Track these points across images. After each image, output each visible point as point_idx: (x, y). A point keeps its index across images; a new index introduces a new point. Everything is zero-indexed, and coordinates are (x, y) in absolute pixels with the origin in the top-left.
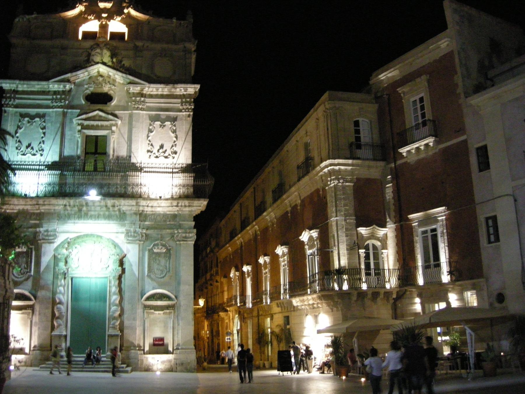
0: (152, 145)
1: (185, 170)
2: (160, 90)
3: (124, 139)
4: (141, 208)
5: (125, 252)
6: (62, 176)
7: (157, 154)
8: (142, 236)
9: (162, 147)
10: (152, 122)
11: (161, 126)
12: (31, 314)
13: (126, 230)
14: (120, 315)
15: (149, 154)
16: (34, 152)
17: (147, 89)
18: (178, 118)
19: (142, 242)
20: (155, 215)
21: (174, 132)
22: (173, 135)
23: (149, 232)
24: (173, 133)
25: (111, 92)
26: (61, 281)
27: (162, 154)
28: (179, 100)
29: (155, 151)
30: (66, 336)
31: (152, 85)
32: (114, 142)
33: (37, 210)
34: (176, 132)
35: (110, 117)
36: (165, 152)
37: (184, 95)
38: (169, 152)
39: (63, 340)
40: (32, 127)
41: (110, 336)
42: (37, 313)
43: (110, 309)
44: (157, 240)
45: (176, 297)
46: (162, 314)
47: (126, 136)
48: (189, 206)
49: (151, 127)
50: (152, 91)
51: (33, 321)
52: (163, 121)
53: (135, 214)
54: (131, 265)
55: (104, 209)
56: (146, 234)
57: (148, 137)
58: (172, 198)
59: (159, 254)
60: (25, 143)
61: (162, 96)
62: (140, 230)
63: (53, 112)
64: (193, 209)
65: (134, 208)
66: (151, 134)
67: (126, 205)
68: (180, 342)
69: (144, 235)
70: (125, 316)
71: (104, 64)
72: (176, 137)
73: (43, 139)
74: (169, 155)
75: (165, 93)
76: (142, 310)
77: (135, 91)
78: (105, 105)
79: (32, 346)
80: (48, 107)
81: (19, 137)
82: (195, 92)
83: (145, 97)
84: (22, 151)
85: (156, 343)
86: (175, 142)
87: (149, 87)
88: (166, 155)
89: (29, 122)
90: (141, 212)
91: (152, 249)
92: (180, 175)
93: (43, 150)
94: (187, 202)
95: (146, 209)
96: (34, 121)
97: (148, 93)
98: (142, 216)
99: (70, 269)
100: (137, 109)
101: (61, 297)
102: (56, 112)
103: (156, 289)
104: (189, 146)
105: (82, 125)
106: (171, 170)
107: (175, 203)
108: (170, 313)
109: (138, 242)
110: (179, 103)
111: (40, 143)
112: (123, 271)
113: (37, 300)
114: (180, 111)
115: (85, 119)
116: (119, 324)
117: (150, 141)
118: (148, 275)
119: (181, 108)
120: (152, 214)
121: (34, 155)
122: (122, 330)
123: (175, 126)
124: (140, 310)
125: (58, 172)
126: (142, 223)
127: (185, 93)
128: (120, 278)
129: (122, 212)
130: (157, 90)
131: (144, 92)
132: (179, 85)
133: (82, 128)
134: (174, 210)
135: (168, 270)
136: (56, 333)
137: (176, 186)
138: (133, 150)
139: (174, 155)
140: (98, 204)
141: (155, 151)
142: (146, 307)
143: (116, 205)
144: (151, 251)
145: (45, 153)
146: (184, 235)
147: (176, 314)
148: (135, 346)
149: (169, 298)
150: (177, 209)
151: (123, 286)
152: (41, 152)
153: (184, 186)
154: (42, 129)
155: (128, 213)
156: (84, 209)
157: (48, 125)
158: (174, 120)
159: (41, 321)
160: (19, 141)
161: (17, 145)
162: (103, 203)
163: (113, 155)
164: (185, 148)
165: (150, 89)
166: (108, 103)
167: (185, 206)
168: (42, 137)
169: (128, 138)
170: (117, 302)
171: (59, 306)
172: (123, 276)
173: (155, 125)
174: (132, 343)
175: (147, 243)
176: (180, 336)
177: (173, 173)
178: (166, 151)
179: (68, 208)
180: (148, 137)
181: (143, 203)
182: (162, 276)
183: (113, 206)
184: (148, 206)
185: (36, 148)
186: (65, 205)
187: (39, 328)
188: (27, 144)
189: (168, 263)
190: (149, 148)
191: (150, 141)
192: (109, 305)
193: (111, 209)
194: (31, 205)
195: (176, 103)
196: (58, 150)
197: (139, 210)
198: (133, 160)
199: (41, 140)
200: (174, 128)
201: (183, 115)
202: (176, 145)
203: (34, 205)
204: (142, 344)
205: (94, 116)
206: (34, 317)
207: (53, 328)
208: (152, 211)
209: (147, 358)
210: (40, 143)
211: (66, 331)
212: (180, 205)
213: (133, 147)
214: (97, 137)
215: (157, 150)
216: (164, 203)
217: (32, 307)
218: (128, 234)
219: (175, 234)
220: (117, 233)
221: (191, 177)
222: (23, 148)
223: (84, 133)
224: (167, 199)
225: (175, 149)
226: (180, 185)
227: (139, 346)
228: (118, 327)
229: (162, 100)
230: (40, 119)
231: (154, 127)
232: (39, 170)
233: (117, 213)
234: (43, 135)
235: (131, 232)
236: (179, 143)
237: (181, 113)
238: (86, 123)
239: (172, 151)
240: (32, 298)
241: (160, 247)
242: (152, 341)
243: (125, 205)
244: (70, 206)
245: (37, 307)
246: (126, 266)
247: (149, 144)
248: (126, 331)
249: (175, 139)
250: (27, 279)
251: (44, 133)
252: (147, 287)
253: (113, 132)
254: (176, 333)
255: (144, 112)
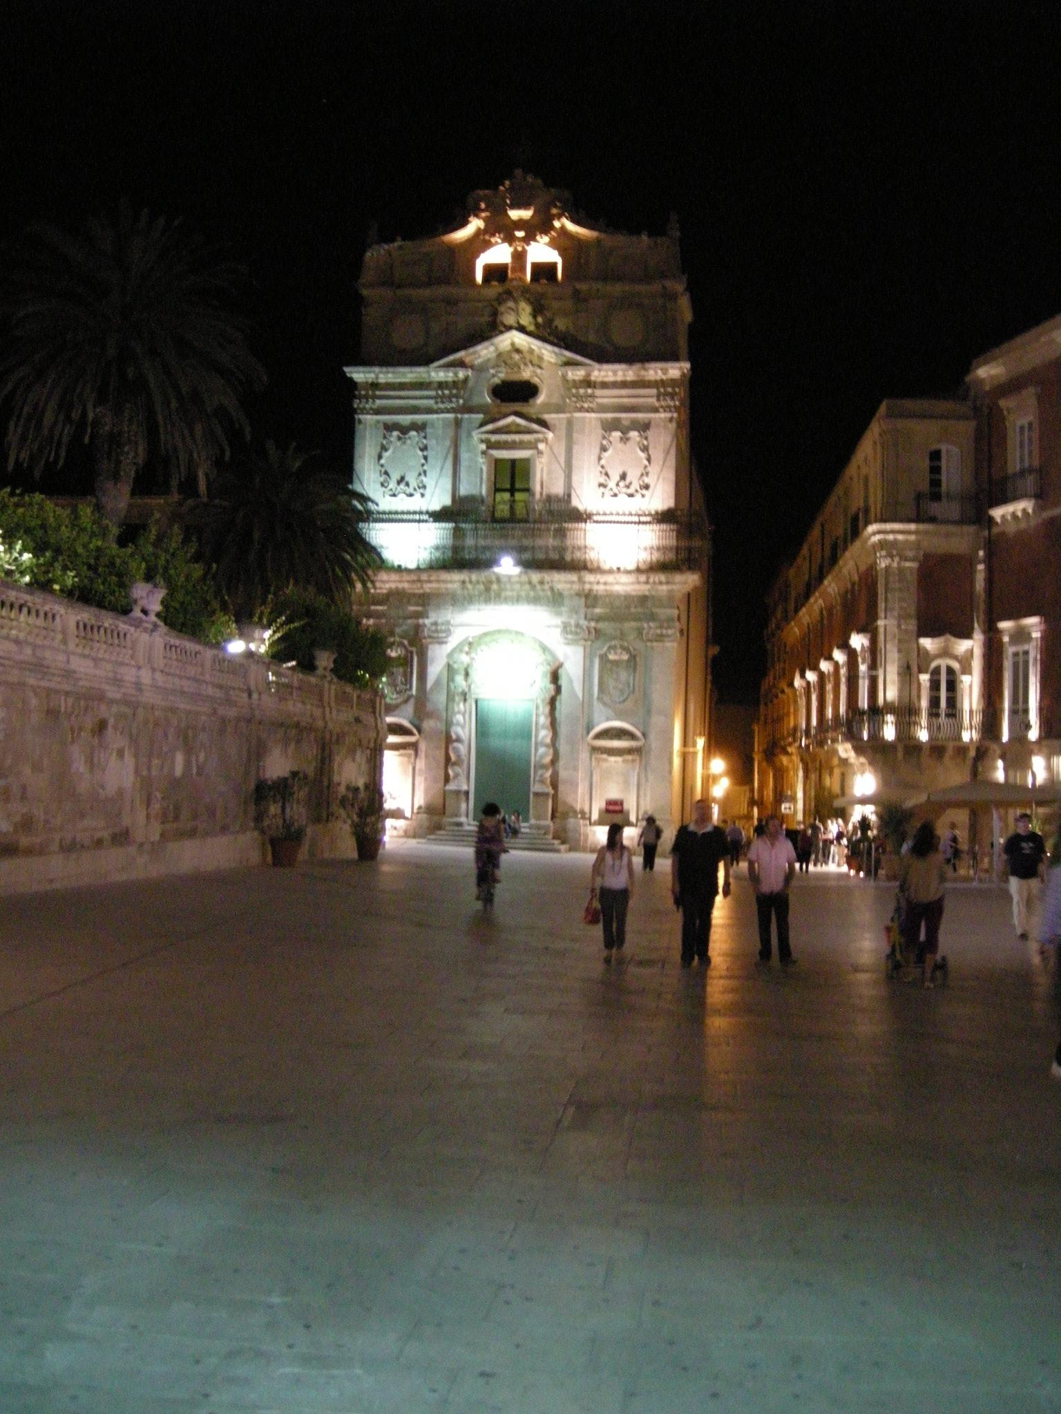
0: (607, 474)
1: (664, 517)
2: (620, 373)
3: (559, 463)
4: (587, 587)
5: (562, 659)
6: (457, 533)
7: (616, 490)
8: (589, 632)
9: (623, 477)
10: (606, 431)
11: (621, 439)
12: (413, 756)
13: (563, 623)
14: (554, 762)
15: (602, 489)
16: (410, 490)
17: (596, 373)
18: (653, 422)
19: (589, 643)
20: (610, 596)
21: (645, 449)
22: (643, 455)
23: (601, 625)
24: (643, 452)
25: (536, 380)
26: (458, 704)
27: (625, 490)
28: (654, 391)
29: (612, 484)
30: (467, 793)
31: (605, 366)
32: (542, 470)
33: (419, 589)
34: (647, 451)
35: (535, 427)
36: (628, 487)
37: (662, 381)
38: (635, 486)
39: (464, 798)
40: (405, 447)
41: (537, 794)
42: (422, 754)
43: (536, 750)
44: (615, 638)
45: (644, 735)
46: (620, 764)
47: (562, 460)
48: (668, 583)
49: (605, 442)
50: (605, 376)
51: (417, 768)
52: (625, 431)
53: (578, 595)
54: (571, 681)
55: (527, 587)
56: (595, 629)
57: (600, 459)
58: (638, 570)
59: (616, 663)
60: (395, 476)
61: (624, 385)
62: (586, 623)
63: (438, 419)
64: (674, 587)
65: (576, 587)
66: (606, 455)
67: (562, 581)
68: (648, 808)
69: (593, 631)
70: (561, 763)
71: (522, 329)
72: (649, 460)
73: (425, 467)
74: (637, 491)
75: (629, 379)
76: (588, 754)
77: (576, 378)
78: (525, 404)
79: (416, 806)
80: (429, 411)
81: (386, 465)
82: (683, 375)
83: (595, 387)
84: (391, 490)
85: (611, 808)
86: (646, 467)
87: (600, 370)
88: (631, 491)
89: (399, 438)
90: (586, 592)
91: (605, 654)
92: (656, 527)
93: (424, 487)
94: (663, 577)
95: (595, 587)
96: (407, 436)
97: (600, 379)
98: (590, 598)
99: (473, 687)
100: (581, 409)
101: (460, 730)
102: (443, 420)
103: (612, 720)
104: (670, 475)
105: (487, 442)
106: (636, 519)
107: (643, 578)
108: (633, 761)
109: (583, 642)
110: (652, 397)
111: (420, 474)
112: (558, 690)
113: (423, 735)
114: (656, 410)
115: (493, 432)
116: (551, 776)
117: (603, 467)
118: (599, 698)
119: (657, 404)
120: (607, 596)
121: (411, 495)
122: (555, 784)
123: (646, 438)
124: (584, 755)
125: (451, 525)
126: (590, 610)
127: (664, 377)
128: (552, 702)
129: (556, 591)
130: (615, 373)
131: (593, 378)
132: (653, 365)
133: (488, 448)
134: (644, 589)
135: (631, 689)
136: (451, 787)
137: (645, 549)
138: (575, 483)
139: (644, 492)
140: (517, 579)
141: (612, 484)
142: (595, 749)
143: (546, 580)
144: (603, 658)
145: (428, 492)
146: (659, 631)
147: (643, 761)
148: (575, 812)
149: (632, 736)
150: (648, 587)
151: (557, 714)
152: (422, 491)
153: (658, 549)
154: (422, 450)
155: (566, 593)
156: (495, 587)
157: (431, 443)
158: (644, 427)
159: (429, 767)
160: (386, 473)
161: (382, 479)
162: (524, 578)
163: (541, 494)
164: (663, 479)
165: (603, 373)
166: (531, 401)
167: (661, 583)
168: (423, 465)
169: (565, 462)
170: (548, 740)
171: (456, 744)
172: (558, 698)
173: (611, 439)
174: (572, 807)
175: (598, 643)
176: (648, 798)
177: (640, 523)
178: (631, 483)
179: (469, 586)
180: (600, 459)
181: (589, 577)
182: (622, 699)
183: (542, 583)
184: (598, 583)
185: (413, 483)
186: (463, 582)
187: (426, 779)
188: (399, 478)
189: (632, 677)
190: (602, 479)
191: (603, 467)
192: (536, 744)
193: (538, 587)
194: (408, 582)
195: (648, 397)
196: (449, 486)
197: (583, 590)
198: (575, 503)
199: (421, 470)
200: (645, 443)
201: (660, 418)
202: (647, 474)
203: (414, 582)
204: (587, 810)
205: (508, 426)
206: (418, 761)
207: (447, 779)
208: (606, 591)
209: (594, 832)
210: (420, 474)
211: (468, 785)
212: (651, 580)
213: (575, 478)
214: (513, 462)
215: (616, 482)
216: (624, 579)
217: (414, 746)
218: (565, 628)
219: (643, 629)
220: (549, 627)
221: (673, 530)
222: (392, 485)
223: (492, 455)
224: (628, 572)
225: (646, 480)
226: (652, 548)
227: (583, 813)
228: (549, 780)
229: (624, 392)
230: (417, 431)
231: (611, 442)
232: (419, 521)
233: (549, 593)
234: (423, 461)
235: (571, 625)
236: (654, 469)
237: (657, 415)
238: (494, 438)
239: (641, 483)
240: (415, 731)
241: (619, 651)
242: (603, 805)
243: (560, 581)
244: (471, 582)
245: (423, 746)
246: (563, 682)
247: (601, 472)
248: (561, 788)
249: (646, 463)
250: (406, 701)
251: (426, 458)
252: (596, 717)
253: (540, 453)
254: (642, 793)
255: (593, 415)
